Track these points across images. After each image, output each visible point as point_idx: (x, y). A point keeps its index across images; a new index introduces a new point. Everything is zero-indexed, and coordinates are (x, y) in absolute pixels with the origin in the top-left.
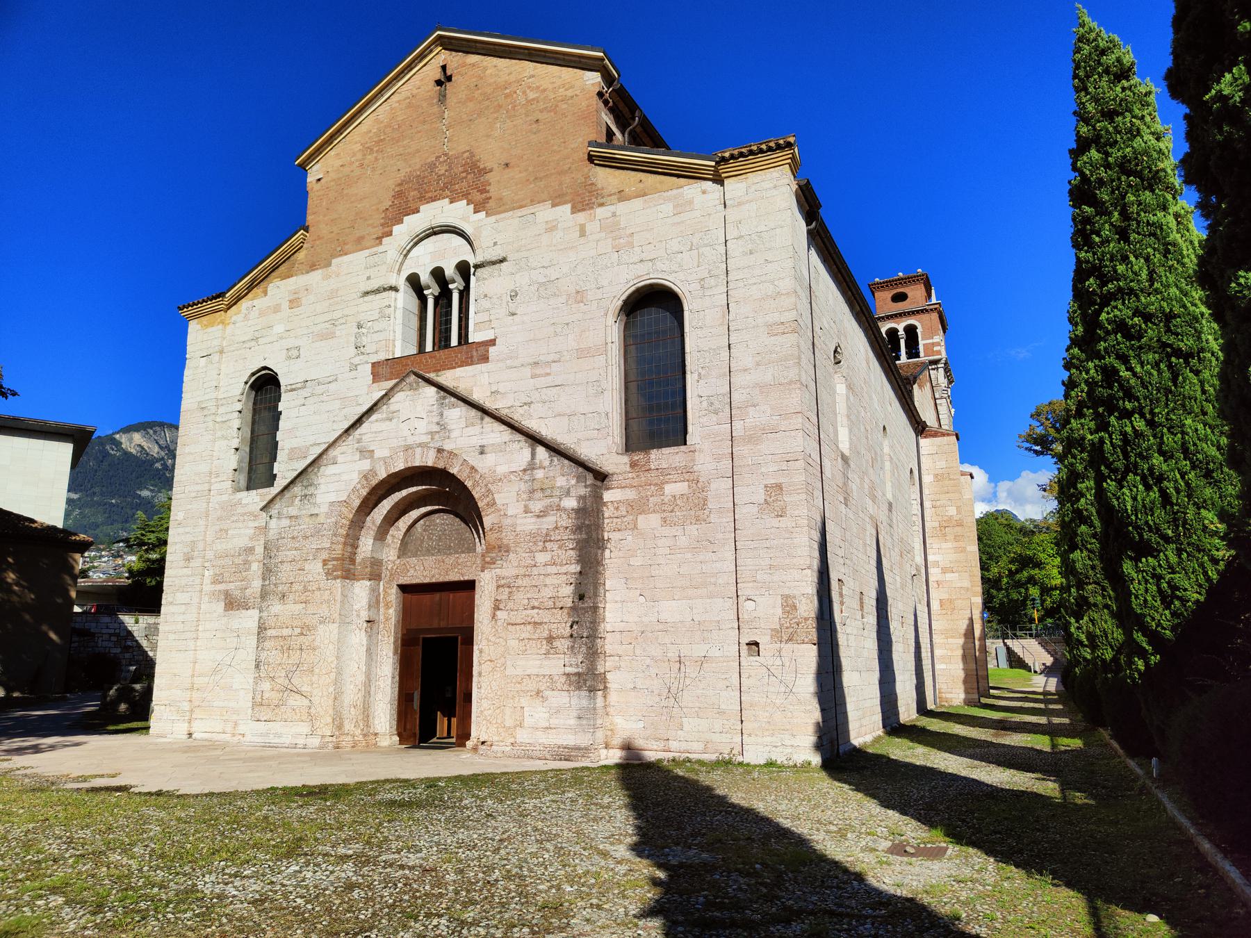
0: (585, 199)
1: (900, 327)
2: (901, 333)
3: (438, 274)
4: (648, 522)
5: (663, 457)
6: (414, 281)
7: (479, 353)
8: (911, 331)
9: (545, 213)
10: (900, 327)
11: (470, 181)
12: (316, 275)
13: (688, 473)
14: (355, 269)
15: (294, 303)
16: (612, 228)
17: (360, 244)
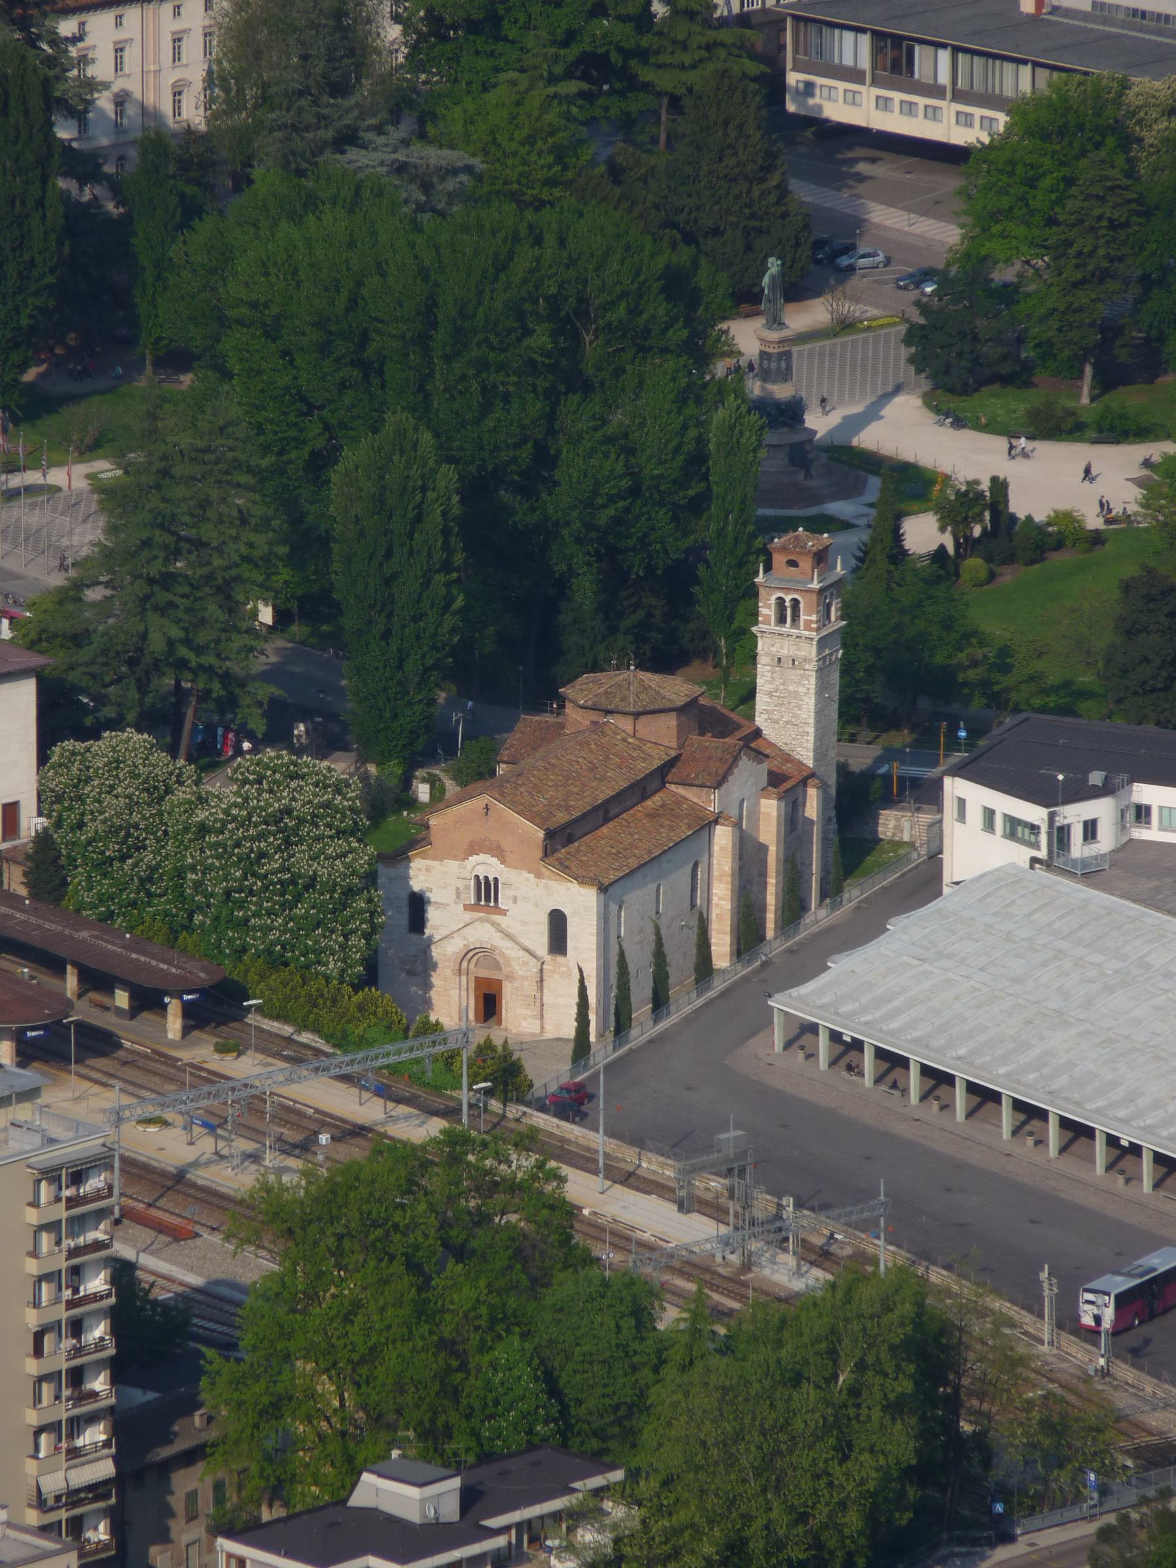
0: (539, 875)
1: (788, 598)
2: (787, 604)
3: (486, 878)
4: (556, 976)
5: (560, 959)
6: (477, 877)
7: (503, 913)
8: (795, 602)
9: (525, 874)
10: (788, 598)
11: (498, 851)
12: (436, 863)
13: (567, 966)
14: (452, 865)
15: (428, 870)
16: (547, 887)
17: (455, 858)
